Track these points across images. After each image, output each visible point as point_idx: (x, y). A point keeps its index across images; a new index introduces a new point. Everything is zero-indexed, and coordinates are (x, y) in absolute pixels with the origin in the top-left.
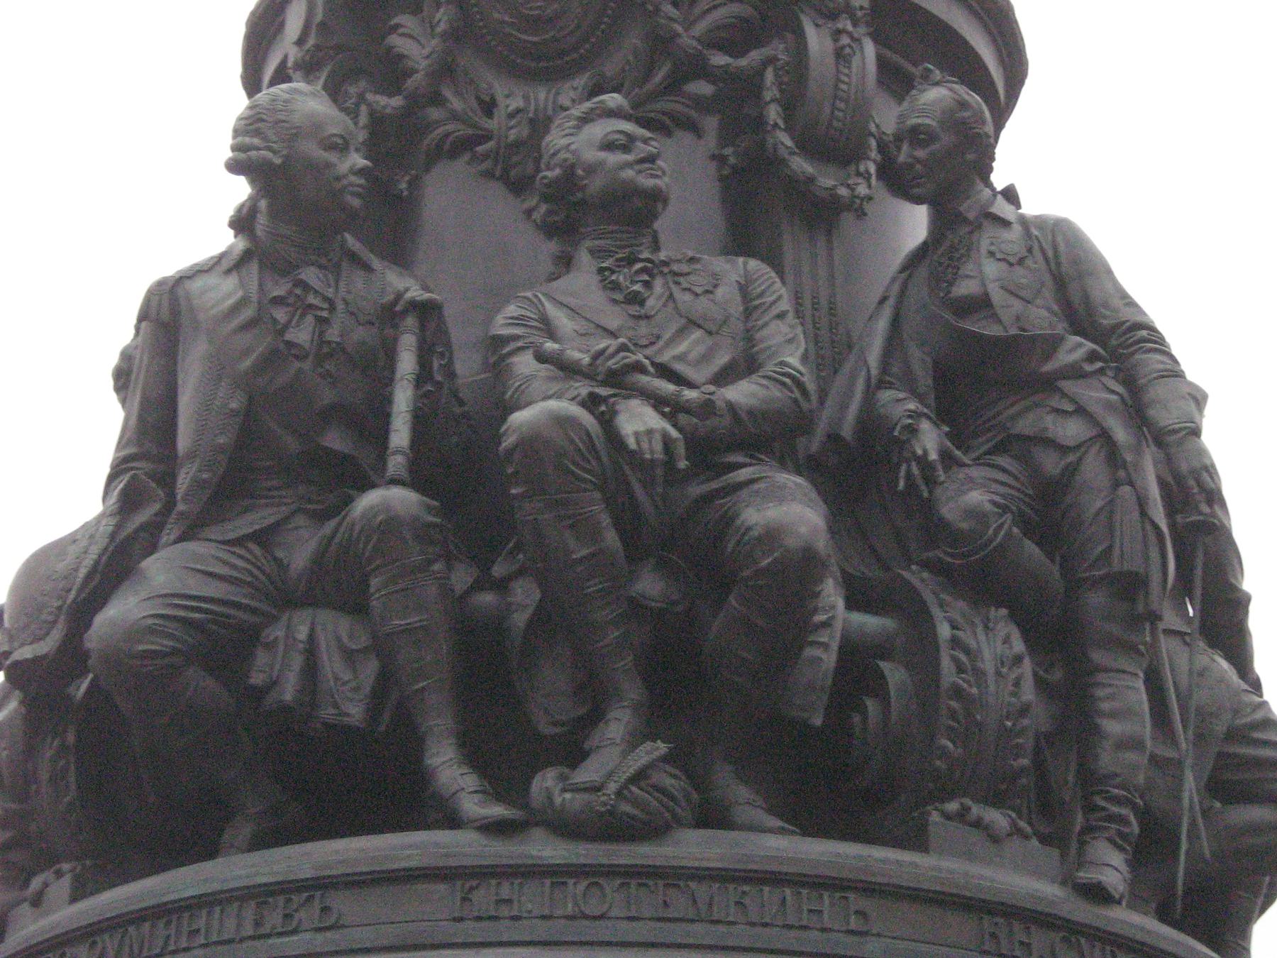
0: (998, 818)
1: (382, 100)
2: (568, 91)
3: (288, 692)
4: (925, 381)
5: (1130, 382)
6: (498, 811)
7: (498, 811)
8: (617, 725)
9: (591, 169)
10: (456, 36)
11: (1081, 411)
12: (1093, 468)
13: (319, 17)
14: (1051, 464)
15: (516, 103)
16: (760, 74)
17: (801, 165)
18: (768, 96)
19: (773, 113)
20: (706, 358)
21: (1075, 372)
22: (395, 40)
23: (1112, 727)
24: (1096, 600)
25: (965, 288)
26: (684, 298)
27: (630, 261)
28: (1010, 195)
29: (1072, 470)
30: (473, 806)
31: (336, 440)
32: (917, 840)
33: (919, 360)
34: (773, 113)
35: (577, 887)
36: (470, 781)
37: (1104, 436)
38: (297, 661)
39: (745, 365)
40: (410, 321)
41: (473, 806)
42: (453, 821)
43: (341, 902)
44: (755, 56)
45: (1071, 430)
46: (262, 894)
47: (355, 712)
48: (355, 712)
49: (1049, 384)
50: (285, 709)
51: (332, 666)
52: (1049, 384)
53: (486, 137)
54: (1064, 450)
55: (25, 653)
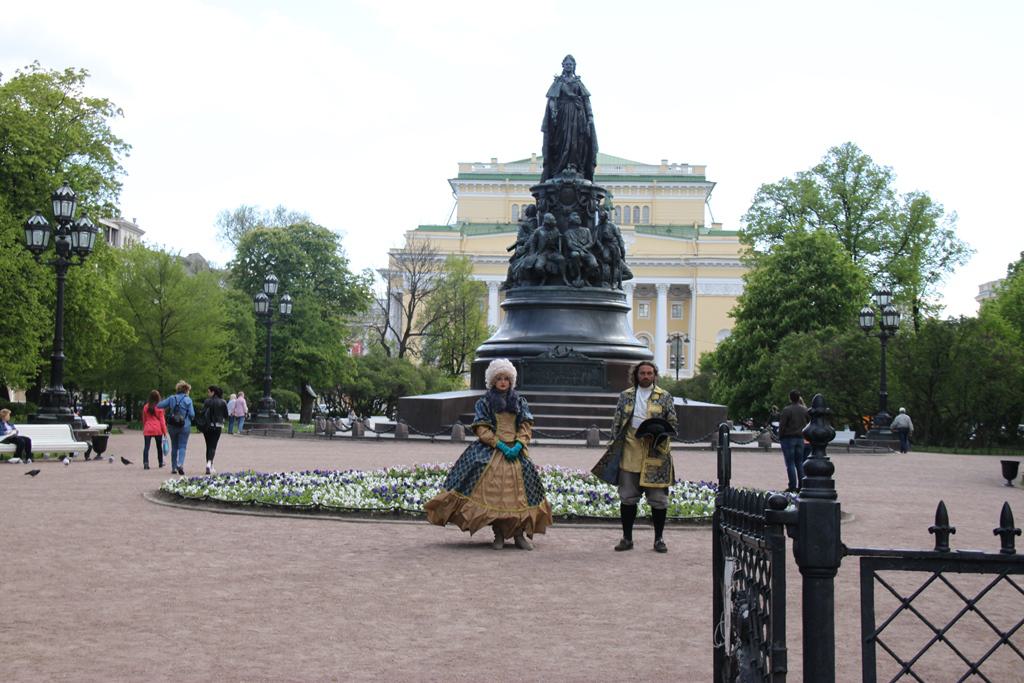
2: (569, 208)
8: (579, 278)
42: (565, 284)
46: (552, 291)
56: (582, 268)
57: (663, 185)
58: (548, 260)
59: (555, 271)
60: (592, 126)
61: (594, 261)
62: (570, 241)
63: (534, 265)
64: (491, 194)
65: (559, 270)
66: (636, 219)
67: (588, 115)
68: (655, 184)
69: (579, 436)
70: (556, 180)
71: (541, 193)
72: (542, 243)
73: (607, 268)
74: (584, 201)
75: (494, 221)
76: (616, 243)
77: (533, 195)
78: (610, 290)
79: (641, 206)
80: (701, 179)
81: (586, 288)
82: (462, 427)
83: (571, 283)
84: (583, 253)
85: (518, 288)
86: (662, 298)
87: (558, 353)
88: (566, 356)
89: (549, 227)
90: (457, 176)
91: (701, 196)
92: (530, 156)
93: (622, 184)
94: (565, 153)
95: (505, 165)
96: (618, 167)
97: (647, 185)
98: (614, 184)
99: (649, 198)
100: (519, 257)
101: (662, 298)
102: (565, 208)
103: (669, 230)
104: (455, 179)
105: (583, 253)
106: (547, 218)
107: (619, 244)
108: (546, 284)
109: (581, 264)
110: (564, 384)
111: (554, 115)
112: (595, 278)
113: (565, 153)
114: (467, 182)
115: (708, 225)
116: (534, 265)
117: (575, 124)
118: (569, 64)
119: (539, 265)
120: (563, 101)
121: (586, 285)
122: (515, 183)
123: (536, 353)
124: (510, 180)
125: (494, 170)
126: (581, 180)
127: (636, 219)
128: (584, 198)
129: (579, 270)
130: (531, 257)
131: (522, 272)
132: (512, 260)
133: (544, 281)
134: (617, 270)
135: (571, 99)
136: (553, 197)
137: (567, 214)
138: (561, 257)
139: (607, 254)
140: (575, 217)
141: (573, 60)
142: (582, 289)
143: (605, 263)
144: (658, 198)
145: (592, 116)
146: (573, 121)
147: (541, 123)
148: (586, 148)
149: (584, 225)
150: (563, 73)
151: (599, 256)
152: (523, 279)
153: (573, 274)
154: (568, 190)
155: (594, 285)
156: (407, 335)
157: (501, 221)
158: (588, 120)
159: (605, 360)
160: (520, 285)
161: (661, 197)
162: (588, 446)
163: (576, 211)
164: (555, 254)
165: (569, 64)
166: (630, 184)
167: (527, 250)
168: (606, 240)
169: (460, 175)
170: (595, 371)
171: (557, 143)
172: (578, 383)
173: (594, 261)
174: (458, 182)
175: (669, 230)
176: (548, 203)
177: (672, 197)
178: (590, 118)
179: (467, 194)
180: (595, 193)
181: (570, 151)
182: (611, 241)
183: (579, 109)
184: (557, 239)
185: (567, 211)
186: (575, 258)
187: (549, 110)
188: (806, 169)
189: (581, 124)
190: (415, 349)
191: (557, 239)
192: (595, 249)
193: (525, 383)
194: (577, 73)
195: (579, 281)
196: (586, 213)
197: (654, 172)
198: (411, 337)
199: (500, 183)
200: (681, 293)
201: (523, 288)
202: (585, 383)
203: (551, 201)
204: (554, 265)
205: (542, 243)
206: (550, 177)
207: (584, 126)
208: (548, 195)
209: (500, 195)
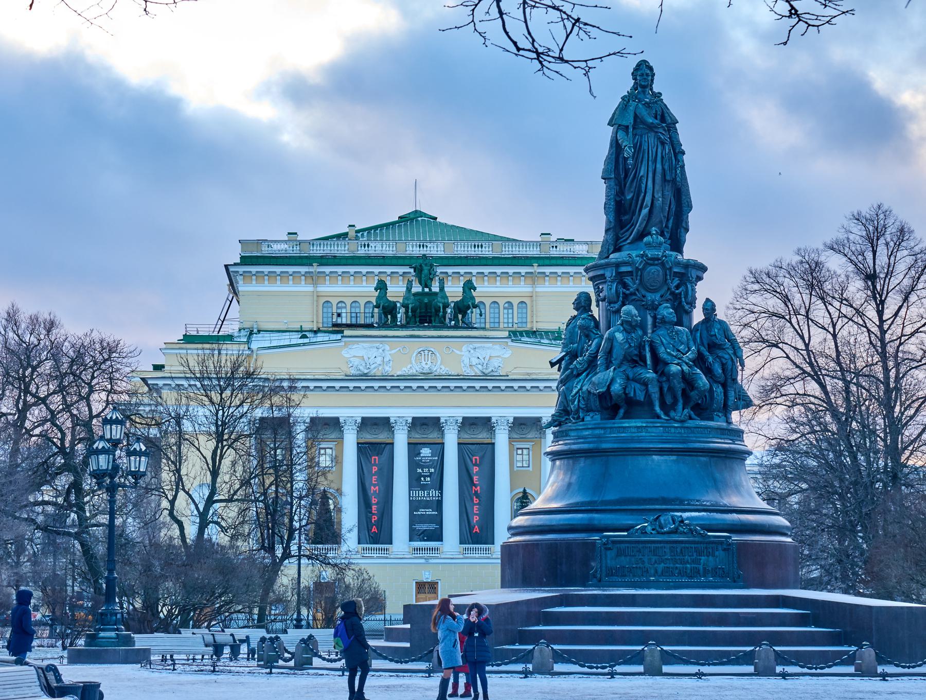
0: (720, 414)
1: (625, 290)
2: (657, 297)
3: (632, 395)
4: (707, 346)
5: (733, 348)
6: (667, 418)
7: (667, 418)
9: (666, 317)
10: (639, 284)
11: (729, 354)
12: (730, 363)
13: (614, 274)
14: (724, 361)
15: (649, 298)
16: (681, 293)
17: (687, 307)
18: (683, 296)
19: (683, 300)
20: (685, 349)
21: (728, 348)
22: (626, 280)
23: (730, 398)
24: (729, 381)
25: (713, 333)
26: (680, 338)
27: (672, 331)
28: (716, 315)
29: (726, 363)
30: (663, 416)
31: (635, 358)
32: (712, 419)
33: (706, 343)
34: (683, 300)
35: (679, 429)
36: (662, 412)
37: (732, 358)
38: (633, 390)
39: (689, 350)
40: (647, 343)
41: (663, 416)
42: (659, 417)
43: (649, 430)
44: (681, 289)
45: (727, 356)
46: (638, 427)
47: (642, 400)
48: (642, 400)
49: (724, 349)
50: (631, 397)
51: (638, 392)
52: (724, 349)
53: (643, 301)
54: (726, 359)
55: (601, 390)
56: (684, 391)
57: (548, 270)
58: (628, 378)
59: (641, 396)
60: (683, 167)
61: (703, 381)
62: (662, 349)
63: (609, 387)
64: (290, 287)
65: (648, 395)
67: (678, 152)
68: (536, 269)
69: (747, 659)
70: (634, 254)
71: (609, 273)
72: (618, 353)
73: (719, 390)
74: (677, 287)
75: (297, 326)
76: (731, 352)
77: (591, 279)
78: (724, 425)
79: (515, 302)
81: (690, 423)
82: (547, 650)
83: (667, 414)
84: (685, 368)
87: (661, 527)
89: (629, 327)
90: (238, 261)
92: (346, 230)
93: (486, 270)
94: (645, 211)
95: (311, 242)
97: (523, 270)
98: (474, 270)
99: (530, 289)
100: (579, 375)
102: (650, 296)
104: (235, 264)
105: (685, 368)
106: (628, 313)
107: (735, 353)
109: (682, 385)
110: (673, 575)
111: (628, 152)
112: (702, 409)
113: (645, 211)
114: (254, 269)
116: (609, 387)
117: (659, 166)
119: (616, 388)
120: (639, 132)
121: (691, 418)
124: (321, 265)
126: (674, 253)
128: (676, 281)
129: (679, 393)
130: (602, 376)
131: (587, 401)
132: (563, 382)
133: (622, 412)
134: (732, 395)
135: (651, 128)
136: (628, 280)
137: (654, 308)
138: (650, 374)
139: (718, 370)
140: (666, 311)
141: (651, 69)
142: (686, 425)
143: (716, 382)
144: (538, 289)
145: (683, 153)
146: (655, 161)
147: (601, 166)
148: (673, 207)
149: (680, 323)
150: (635, 88)
151: (708, 372)
152: (588, 410)
153: (669, 400)
154: (653, 269)
155: (702, 419)
156: (210, 501)
157: (307, 326)
158: (677, 160)
159: (735, 538)
162: (758, 673)
163: (667, 301)
164: (639, 370)
166: (499, 270)
167: (591, 365)
168: (713, 347)
169: (242, 258)
170: (720, 553)
171: (629, 197)
172: (695, 573)
173: (703, 381)
174: (241, 269)
176: (621, 290)
178: (679, 156)
180: (694, 273)
181: (651, 212)
182: (720, 347)
183: (663, 143)
184: (641, 347)
185: (653, 302)
186: (674, 375)
187: (616, 146)
189: (666, 167)
190: (223, 524)
191: (641, 347)
192: (700, 360)
194: (656, 89)
195: (680, 412)
196: (680, 302)
197: (534, 252)
198: (217, 505)
202: (706, 573)
203: (625, 286)
204: (638, 386)
205: (618, 353)
206: (618, 249)
207: (673, 169)
208: (620, 278)
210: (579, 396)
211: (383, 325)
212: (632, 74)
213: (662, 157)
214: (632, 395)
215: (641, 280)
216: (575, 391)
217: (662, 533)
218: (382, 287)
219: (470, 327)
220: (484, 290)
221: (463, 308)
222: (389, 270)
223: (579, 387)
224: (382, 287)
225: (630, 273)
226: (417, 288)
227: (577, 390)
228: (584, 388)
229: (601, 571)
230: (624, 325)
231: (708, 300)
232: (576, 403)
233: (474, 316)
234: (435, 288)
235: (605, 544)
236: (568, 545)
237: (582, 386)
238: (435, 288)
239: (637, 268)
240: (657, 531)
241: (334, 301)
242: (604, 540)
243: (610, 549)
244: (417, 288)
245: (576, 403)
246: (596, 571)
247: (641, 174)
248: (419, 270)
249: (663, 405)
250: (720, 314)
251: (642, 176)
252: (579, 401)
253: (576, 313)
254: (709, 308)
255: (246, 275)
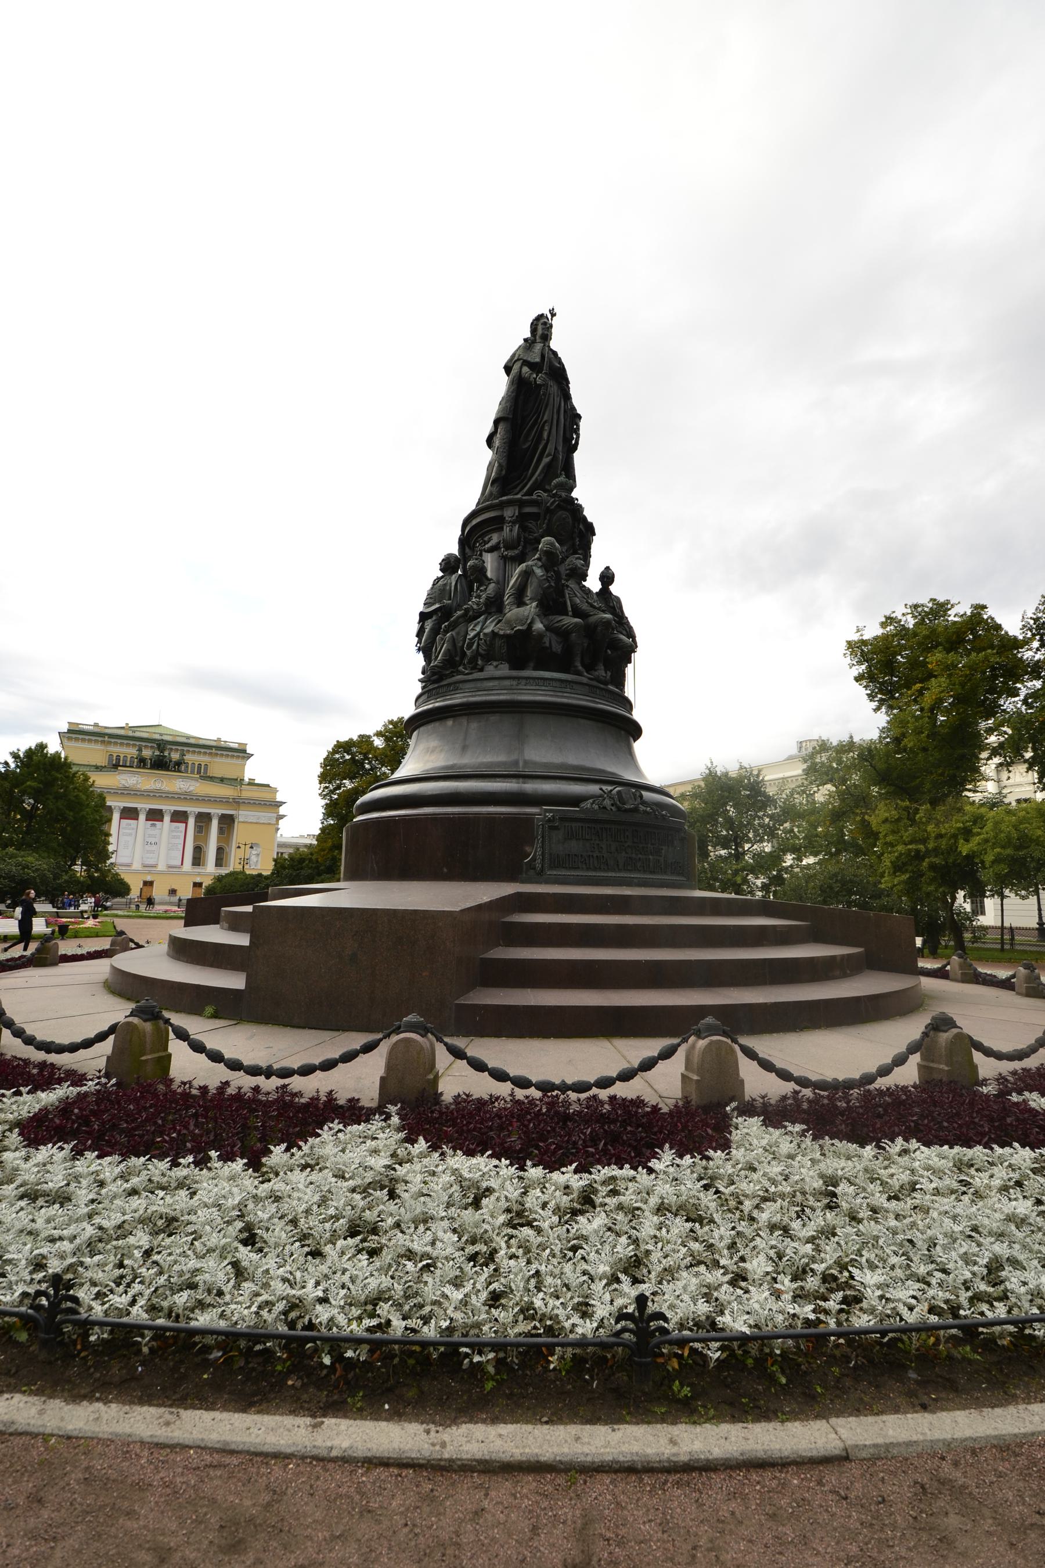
3: (547, 644)
42: (579, 674)
43: (575, 686)
59: (557, 648)
64: (93, 746)
66: (199, 772)
80: (244, 751)
85: (477, 675)
86: (215, 823)
88: (635, 810)
91: (239, 761)
93: (191, 749)
96: (188, 738)
101: (215, 823)
103: (222, 780)
108: (535, 669)
110: (635, 869)
113: (546, 460)
115: (246, 779)
118: (541, 328)
122: (113, 740)
123: (575, 800)
125: (96, 730)
127: (199, 772)
133: (532, 665)
136: (531, 525)
152: (488, 658)
160: (481, 670)
161: (218, 760)
165: (541, 328)
175: (222, 780)
177: (224, 760)
179: (73, 744)
188: (370, 732)
193: (551, 868)
197: (214, 744)
199: (100, 739)
200: (227, 822)
201: (490, 670)
209: (99, 747)
210: (480, 639)
211: (139, 767)
212: (532, 324)
213: (565, 411)
214: (547, 644)
215: (548, 525)
216: (472, 634)
217: (626, 811)
218: (140, 750)
219: (180, 771)
220: (189, 758)
221: (178, 764)
222: (144, 744)
223: (478, 629)
224: (140, 750)
225: (535, 516)
226: (157, 753)
227: (474, 633)
228: (487, 630)
229: (543, 860)
230: (544, 558)
231: (608, 568)
232: (474, 647)
233: (183, 768)
234: (166, 754)
235: (549, 820)
236: (491, 818)
237: (482, 629)
238: (166, 754)
239: (548, 508)
240: (619, 809)
241: (115, 755)
242: (549, 815)
243: (556, 828)
244: (157, 753)
245: (474, 647)
246: (534, 859)
247: (545, 418)
248: (159, 745)
249: (583, 665)
250: (614, 589)
251: (546, 422)
252: (478, 644)
253: (441, 574)
254: (607, 578)
255: (69, 739)
